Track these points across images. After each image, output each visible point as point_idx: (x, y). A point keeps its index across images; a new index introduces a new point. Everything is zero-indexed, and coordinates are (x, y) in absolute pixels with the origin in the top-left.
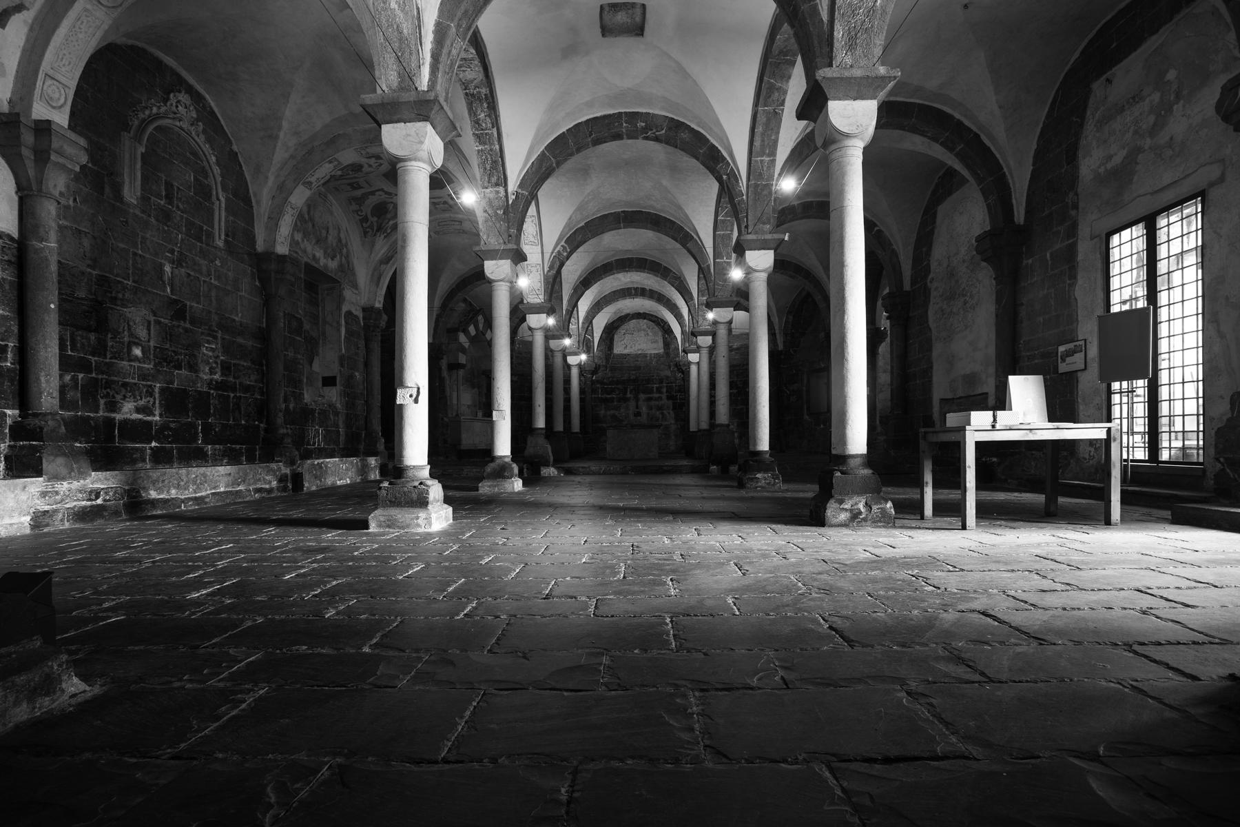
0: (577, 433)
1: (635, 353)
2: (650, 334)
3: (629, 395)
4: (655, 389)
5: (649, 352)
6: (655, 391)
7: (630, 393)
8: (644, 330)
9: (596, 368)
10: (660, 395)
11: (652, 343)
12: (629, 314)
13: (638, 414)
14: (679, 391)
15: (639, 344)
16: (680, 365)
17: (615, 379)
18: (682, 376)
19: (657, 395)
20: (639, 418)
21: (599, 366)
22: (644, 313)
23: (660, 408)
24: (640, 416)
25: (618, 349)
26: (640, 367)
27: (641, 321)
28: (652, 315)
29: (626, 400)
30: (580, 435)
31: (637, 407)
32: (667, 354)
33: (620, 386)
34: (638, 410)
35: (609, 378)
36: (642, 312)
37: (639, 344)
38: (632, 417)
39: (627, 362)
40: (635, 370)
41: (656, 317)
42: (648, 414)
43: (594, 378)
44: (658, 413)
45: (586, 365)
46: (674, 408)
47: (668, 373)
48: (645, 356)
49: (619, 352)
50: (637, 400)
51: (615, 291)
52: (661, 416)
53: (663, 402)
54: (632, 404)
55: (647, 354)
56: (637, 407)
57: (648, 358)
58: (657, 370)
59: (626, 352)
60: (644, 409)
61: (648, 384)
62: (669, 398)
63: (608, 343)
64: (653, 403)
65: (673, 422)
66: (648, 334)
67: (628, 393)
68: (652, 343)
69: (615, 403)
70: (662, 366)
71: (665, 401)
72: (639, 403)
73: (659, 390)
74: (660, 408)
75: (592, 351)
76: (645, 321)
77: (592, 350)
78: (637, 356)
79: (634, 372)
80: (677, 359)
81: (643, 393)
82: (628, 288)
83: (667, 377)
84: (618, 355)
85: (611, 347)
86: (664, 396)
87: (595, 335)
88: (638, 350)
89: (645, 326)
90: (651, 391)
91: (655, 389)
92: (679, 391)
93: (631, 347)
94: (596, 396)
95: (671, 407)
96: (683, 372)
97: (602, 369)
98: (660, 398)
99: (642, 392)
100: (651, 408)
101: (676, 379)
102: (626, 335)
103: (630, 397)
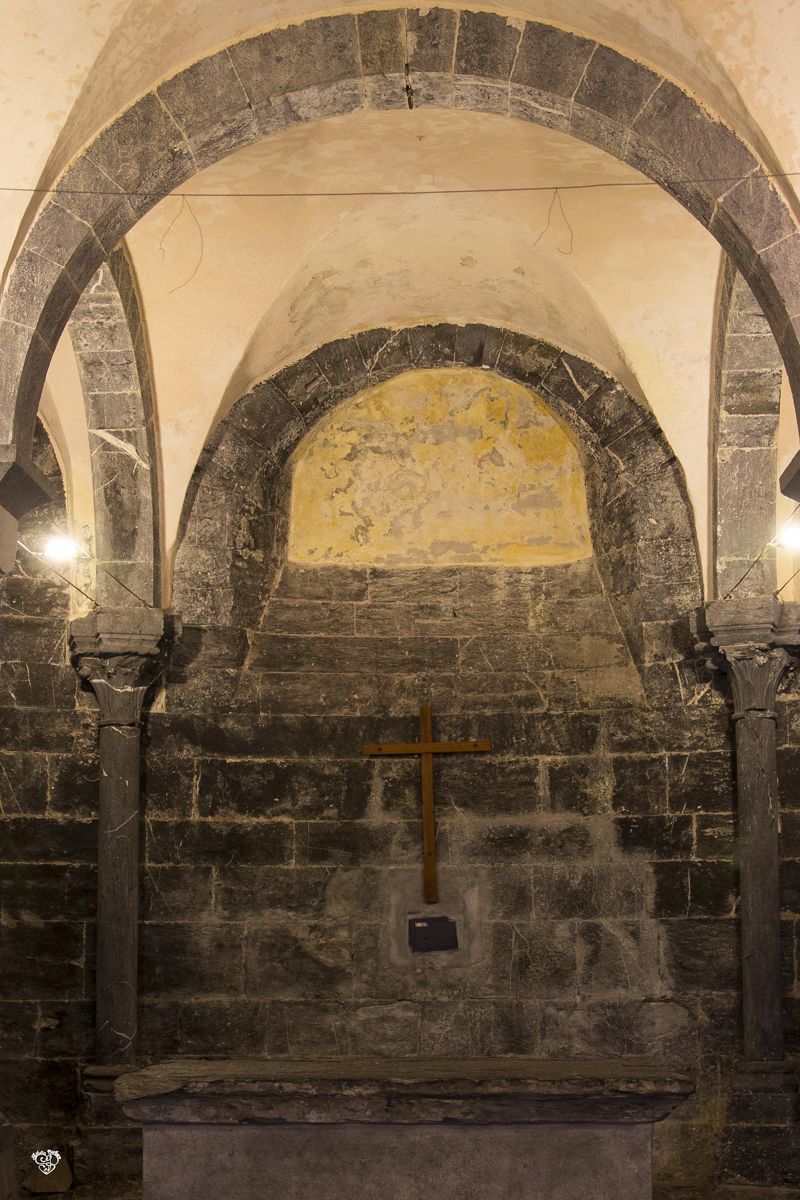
1: (417, 565)
2: (511, 454)
4: (542, 780)
6: (543, 792)
7: (387, 806)
8: (474, 433)
9: (167, 639)
10: (581, 819)
11: (520, 507)
12: (381, 335)
15: (444, 514)
16: (706, 634)
17: (289, 717)
18: (718, 700)
20: (442, 958)
21: (195, 631)
22: (473, 328)
24: (451, 944)
26: (448, 650)
27: (454, 372)
28: (522, 342)
31: (430, 893)
34: (433, 911)
35: (254, 708)
36: (460, 321)
37: (444, 514)
39: (367, 615)
40: (416, 665)
41: (547, 350)
42: (501, 937)
43: (159, 706)
44: (562, 929)
45: (102, 624)
49: (318, 561)
51: (265, 38)
52: (580, 951)
53: (581, 865)
55: (491, 572)
56: (430, 893)
57: (500, 595)
58: (557, 664)
61: (500, 748)
63: (254, 499)
65: (660, 988)
66: (495, 457)
67: (376, 799)
69: (293, 864)
70: (586, 641)
72: (441, 865)
75: (144, 540)
76: (480, 377)
77: (144, 528)
79: (410, 678)
80: (685, 600)
81: (470, 802)
82: (371, 19)
84: (312, 576)
87: (168, 440)
88: (439, 547)
89: (478, 412)
91: (542, 780)
93: (394, 531)
94: (170, 818)
95: (650, 900)
97: (205, 653)
99: (464, 804)
101: (679, 723)
102: (367, 465)
103: (388, 830)
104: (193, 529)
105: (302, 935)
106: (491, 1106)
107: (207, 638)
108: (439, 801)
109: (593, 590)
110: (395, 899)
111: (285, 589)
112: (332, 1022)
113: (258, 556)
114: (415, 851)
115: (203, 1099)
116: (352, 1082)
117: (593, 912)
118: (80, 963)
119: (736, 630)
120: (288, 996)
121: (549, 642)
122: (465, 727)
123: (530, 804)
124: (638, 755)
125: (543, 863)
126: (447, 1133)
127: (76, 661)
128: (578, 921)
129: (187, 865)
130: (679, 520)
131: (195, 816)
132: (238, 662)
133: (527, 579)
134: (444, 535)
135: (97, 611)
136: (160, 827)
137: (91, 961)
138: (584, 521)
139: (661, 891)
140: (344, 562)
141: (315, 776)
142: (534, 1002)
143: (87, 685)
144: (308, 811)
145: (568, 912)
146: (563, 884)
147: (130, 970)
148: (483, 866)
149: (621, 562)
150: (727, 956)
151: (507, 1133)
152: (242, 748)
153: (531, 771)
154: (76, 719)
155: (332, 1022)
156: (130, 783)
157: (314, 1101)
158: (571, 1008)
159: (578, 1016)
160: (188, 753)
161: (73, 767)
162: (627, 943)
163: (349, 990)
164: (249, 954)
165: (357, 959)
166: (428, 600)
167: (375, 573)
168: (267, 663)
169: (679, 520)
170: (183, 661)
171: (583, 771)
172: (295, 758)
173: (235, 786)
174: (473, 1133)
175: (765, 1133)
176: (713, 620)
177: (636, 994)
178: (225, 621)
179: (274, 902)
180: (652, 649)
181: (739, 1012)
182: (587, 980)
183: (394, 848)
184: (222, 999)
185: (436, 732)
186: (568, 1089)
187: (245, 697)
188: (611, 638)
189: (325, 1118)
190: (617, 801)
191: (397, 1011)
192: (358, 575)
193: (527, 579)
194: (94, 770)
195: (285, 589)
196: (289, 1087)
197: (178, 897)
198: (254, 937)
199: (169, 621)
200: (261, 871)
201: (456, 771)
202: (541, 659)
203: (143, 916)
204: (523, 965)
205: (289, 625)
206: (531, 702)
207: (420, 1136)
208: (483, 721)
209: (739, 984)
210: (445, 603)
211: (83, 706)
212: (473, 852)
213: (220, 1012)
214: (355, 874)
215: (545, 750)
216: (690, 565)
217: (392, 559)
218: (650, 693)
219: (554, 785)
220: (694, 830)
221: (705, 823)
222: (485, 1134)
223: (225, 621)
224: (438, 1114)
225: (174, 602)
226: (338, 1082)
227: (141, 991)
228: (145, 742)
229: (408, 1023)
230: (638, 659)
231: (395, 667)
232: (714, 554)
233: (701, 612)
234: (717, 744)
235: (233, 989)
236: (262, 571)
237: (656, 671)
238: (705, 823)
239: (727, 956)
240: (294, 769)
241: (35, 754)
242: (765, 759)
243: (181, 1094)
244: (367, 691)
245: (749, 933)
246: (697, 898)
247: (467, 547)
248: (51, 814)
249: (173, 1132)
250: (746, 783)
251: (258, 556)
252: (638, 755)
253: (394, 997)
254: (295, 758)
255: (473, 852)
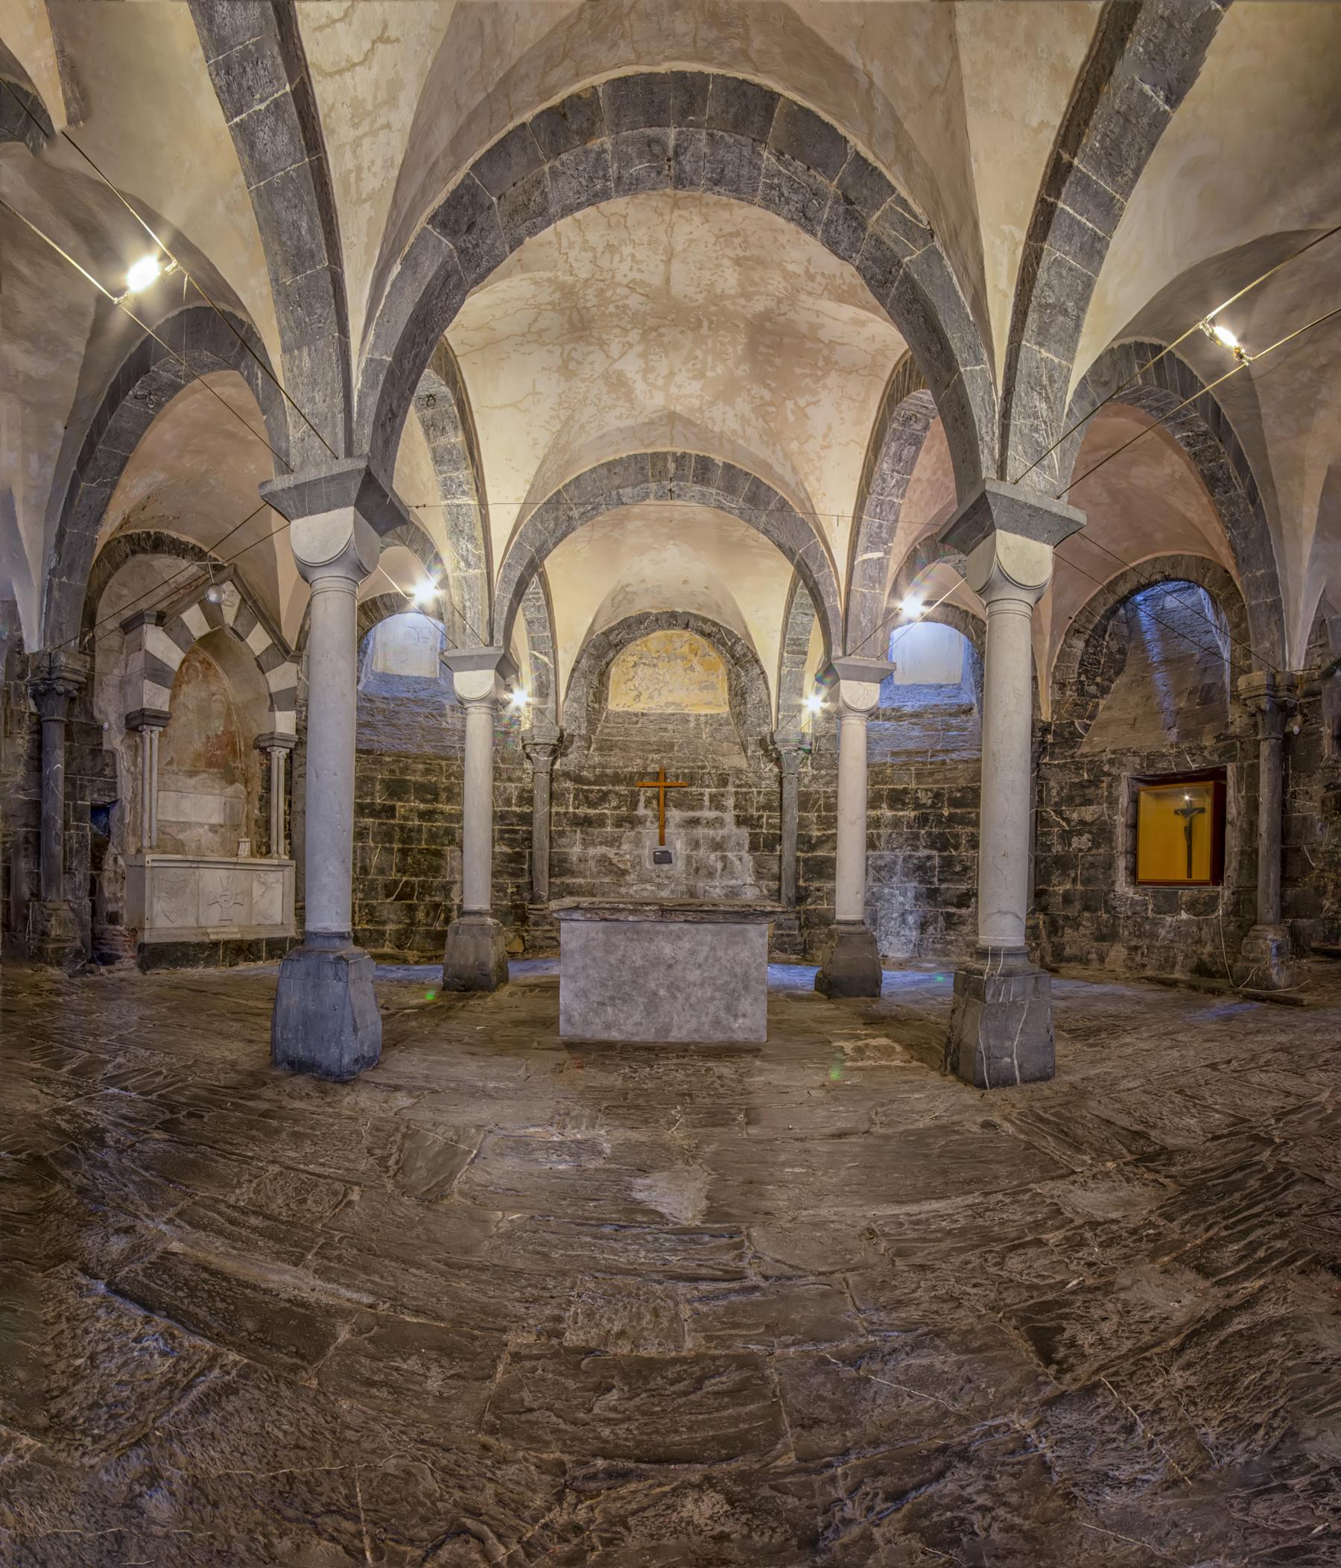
0: (479, 913)
3: (641, 811)
4: (706, 798)
5: (693, 711)
6: (707, 803)
7: (646, 807)
9: (561, 739)
13: (663, 858)
14: (767, 807)
16: (773, 743)
17: (608, 771)
18: (776, 770)
19: (712, 814)
20: (666, 867)
23: (718, 846)
24: (670, 862)
25: (619, 701)
26: (671, 746)
29: (634, 822)
30: (490, 921)
31: (662, 841)
32: (739, 717)
33: (622, 789)
38: (649, 864)
39: (640, 731)
40: (659, 751)
42: (689, 859)
43: (557, 766)
44: (713, 857)
46: (754, 847)
47: (740, 762)
48: (685, 719)
49: (619, 709)
50: (663, 823)
52: (719, 865)
53: (721, 832)
54: (650, 833)
56: (662, 841)
57: (692, 725)
59: (638, 707)
60: (679, 846)
61: (691, 785)
62: (740, 821)
64: (701, 832)
65: (749, 880)
67: (642, 804)
68: (700, 689)
69: (609, 829)
70: (725, 744)
71: (730, 829)
73: (717, 802)
74: (718, 846)
78: (666, 718)
80: (765, 729)
81: (678, 806)
83: (739, 771)
84: (617, 714)
85: (600, 694)
86: (729, 817)
88: (668, 704)
90: (696, 803)
91: (706, 798)
92: (767, 807)
94: (562, 810)
95: (747, 846)
96: (778, 761)
97: (575, 745)
98: (719, 822)
100: (696, 845)
101: (760, 778)
103: (646, 816)
104: (570, 696)
105: (612, 856)
106: (704, 915)
107: (576, 739)
108: (666, 805)
109: (728, 724)
110: (648, 843)
111: (607, 720)
112: (623, 890)
113: (597, 706)
114: (657, 824)
115: (586, 910)
116: (647, 904)
117: (725, 850)
118: (526, 867)
119: (785, 741)
120: (606, 880)
121: (710, 744)
122: (677, 776)
123: (701, 808)
124: (744, 790)
125: (706, 831)
126: (686, 926)
127: (524, 747)
128: (719, 854)
129: (568, 829)
130: (765, 698)
131: (571, 810)
132: (589, 749)
133: (703, 719)
134: (670, 700)
135: (533, 727)
136: (557, 814)
137: (530, 866)
138: (727, 697)
139: (751, 843)
140: (630, 710)
141: (616, 794)
142: (701, 884)
143: (528, 757)
144: (615, 808)
145: (715, 850)
146: (713, 839)
147: (546, 869)
148: (682, 831)
149: (740, 713)
150: (775, 869)
151: (710, 927)
152: (590, 783)
153: (701, 794)
154: (524, 771)
155: (623, 890)
156: (546, 796)
157: (631, 912)
158: (715, 887)
159: (718, 890)
160: (569, 784)
161: (523, 790)
162: (737, 863)
163: (630, 878)
164: (592, 863)
165: (633, 866)
166: (663, 726)
167: (643, 714)
168: (600, 749)
169: (765, 698)
170: (566, 748)
171: (723, 795)
172: (610, 787)
173: (587, 798)
174: (696, 926)
175: (789, 935)
176: (777, 738)
177: (740, 882)
178: (583, 732)
179: (601, 843)
180: (751, 748)
181: (779, 890)
182: (721, 876)
183: (648, 824)
184: (581, 881)
185: (666, 778)
186: (736, 909)
187: (591, 763)
188: (735, 743)
189: (636, 919)
190: (736, 807)
191: (648, 887)
192: (636, 715)
193: (703, 719)
194: (531, 791)
195: (607, 720)
196: (622, 906)
197: (564, 841)
198: (593, 857)
199: (562, 731)
200: (596, 831)
201: (673, 794)
202: (708, 750)
203: (551, 848)
204: (697, 870)
205: (608, 734)
206: (703, 767)
207: (673, 927)
208: (684, 774)
209: (780, 879)
210: (670, 727)
211: (527, 765)
212: (679, 826)
213: (580, 886)
214: (633, 833)
215: (708, 786)
216: (768, 716)
217: (650, 708)
218: (750, 766)
219: (711, 801)
220: (764, 820)
221: (769, 817)
222: (701, 927)
223: (583, 732)
224: (683, 918)
225: (563, 723)
226: (642, 904)
227: (550, 877)
228: (552, 780)
229: (652, 892)
230: (745, 751)
231: (650, 752)
232: (778, 711)
233: (772, 734)
234: (775, 787)
235: (585, 877)
236: (599, 712)
237: (752, 757)
238: (769, 817)
239: (775, 869)
240: (610, 791)
241: (507, 784)
242: (794, 793)
243: (577, 908)
244: (639, 761)
245: (784, 860)
246: (765, 846)
247: (679, 705)
248: (514, 808)
249: (573, 924)
250: (785, 803)
251: (597, 706)
252: (744, 790)
253: (647, 881)
254: (610, 787)
255: (679, 826)
